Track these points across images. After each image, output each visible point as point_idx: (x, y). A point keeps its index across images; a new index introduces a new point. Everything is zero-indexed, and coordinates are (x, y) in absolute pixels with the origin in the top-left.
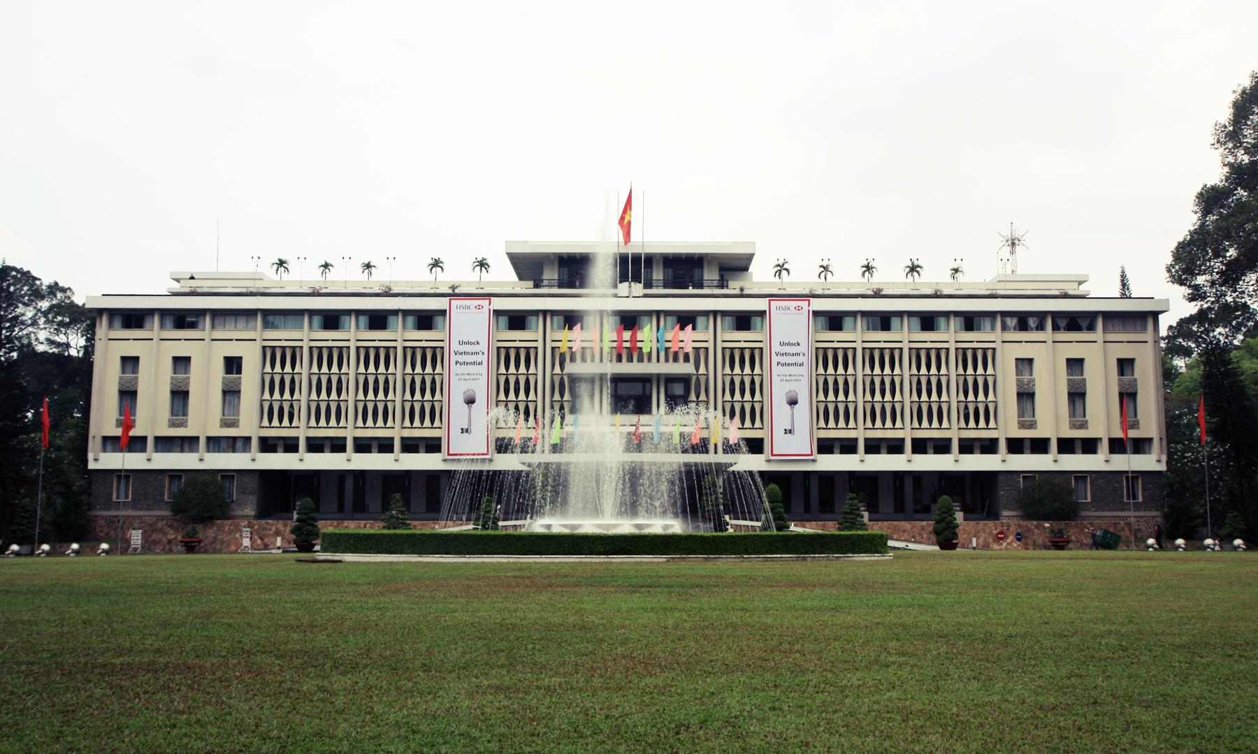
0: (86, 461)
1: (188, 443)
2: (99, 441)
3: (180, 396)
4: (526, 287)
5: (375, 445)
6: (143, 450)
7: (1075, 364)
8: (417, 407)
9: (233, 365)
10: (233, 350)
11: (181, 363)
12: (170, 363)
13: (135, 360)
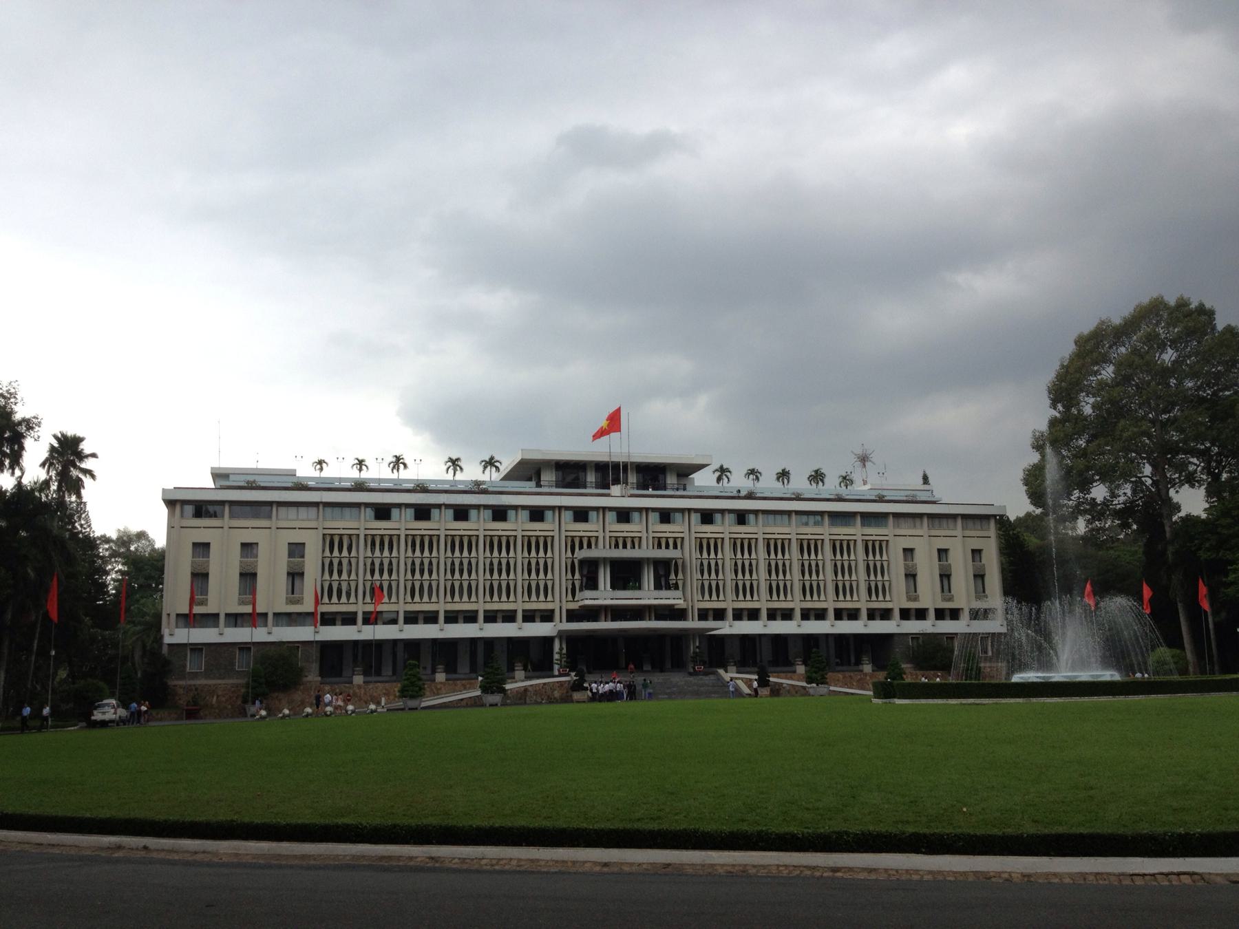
0: (162, 637)
1: (255, 619)
2: (173, 617)
3: (248, 577)
4: (529, 486)
5: (421, 617)
6: (217, 626)
7: (943, 553)
8: (457, 585)
9: (296, 550)
10: (296, 537)
11: (248, 548)
12: (239, 547)
13: (207, 546)
